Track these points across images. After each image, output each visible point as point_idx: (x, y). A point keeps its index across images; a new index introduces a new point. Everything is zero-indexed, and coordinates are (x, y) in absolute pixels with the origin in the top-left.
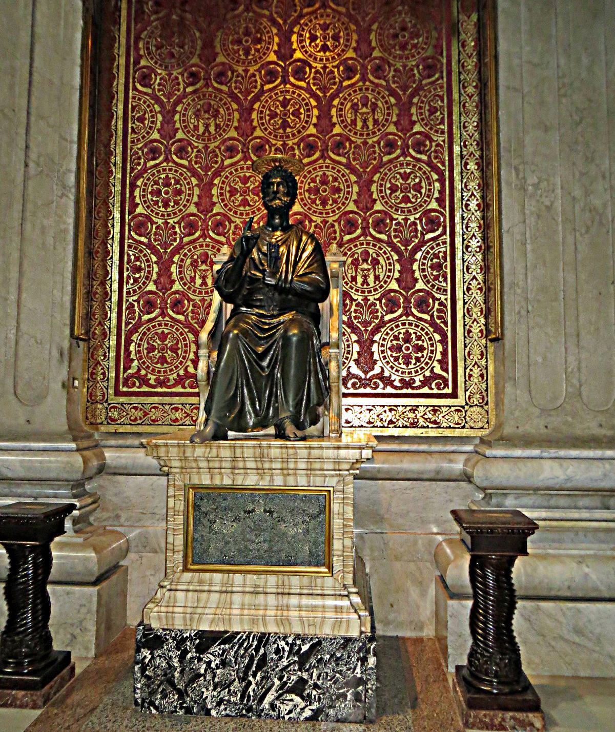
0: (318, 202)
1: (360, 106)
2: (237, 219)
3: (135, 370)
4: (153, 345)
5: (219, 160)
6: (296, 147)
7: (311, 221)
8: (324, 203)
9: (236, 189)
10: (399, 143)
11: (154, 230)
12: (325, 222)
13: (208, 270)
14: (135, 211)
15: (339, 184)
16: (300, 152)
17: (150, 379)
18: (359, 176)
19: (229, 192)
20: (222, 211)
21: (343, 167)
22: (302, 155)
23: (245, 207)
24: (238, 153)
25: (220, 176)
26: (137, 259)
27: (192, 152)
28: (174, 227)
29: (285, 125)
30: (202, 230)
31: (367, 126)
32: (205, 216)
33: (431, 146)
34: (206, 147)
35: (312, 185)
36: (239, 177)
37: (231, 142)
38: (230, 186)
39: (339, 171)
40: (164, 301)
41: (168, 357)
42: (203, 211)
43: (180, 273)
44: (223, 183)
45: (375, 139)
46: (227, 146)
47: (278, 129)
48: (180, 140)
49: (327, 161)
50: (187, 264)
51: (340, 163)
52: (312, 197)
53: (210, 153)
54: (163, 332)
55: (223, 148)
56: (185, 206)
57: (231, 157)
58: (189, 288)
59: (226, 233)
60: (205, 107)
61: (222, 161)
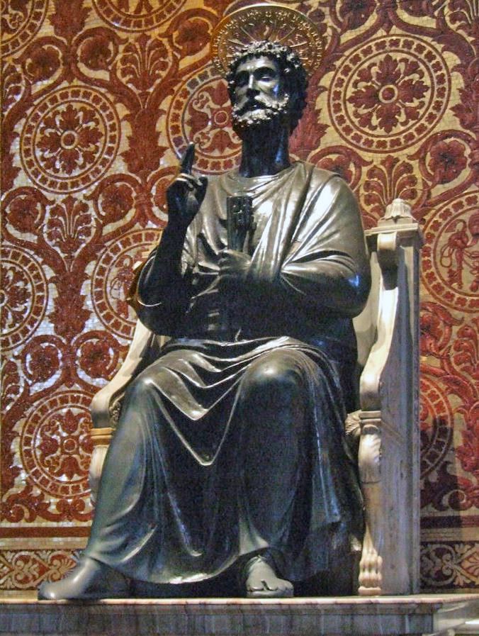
0: (375, 121)
3: (22, 489)
4: (53, 440)
5: (169, 60)
6: (326, 10)
7: (360, 163)
8: (388, 120)
11: (48, 216)
12: (391, 163)
14: (12, 184)
15: (422, 75)
17: (49, 504)
19: (191, 123)
21: (429, 39)
22: (339, 24)
23: (222, 150)
26: (19, 276)
27: (117, 53)
28: (85, 208)
30: (138, 206)
32: (144, 178)
34: (143, 38)
35: (362, 85)
36: (209, 90)
37: (192, 19)
38: (192, 111)
39: (420, 49)
40: (70, 353)
41: (79, 461)
42: (141, 167)
43: (99, 296)
44: (179, 105)
46: (185, 30)
48: (92, 32)
49: (395, 29)
50: (111, 277)
51: (421, 30)
52: (363, 111)
54: (69, 412)
55: (175, 34)
56: (104, 162)
57: (193, 52)
58: (117, 325)
61: (176, 62)
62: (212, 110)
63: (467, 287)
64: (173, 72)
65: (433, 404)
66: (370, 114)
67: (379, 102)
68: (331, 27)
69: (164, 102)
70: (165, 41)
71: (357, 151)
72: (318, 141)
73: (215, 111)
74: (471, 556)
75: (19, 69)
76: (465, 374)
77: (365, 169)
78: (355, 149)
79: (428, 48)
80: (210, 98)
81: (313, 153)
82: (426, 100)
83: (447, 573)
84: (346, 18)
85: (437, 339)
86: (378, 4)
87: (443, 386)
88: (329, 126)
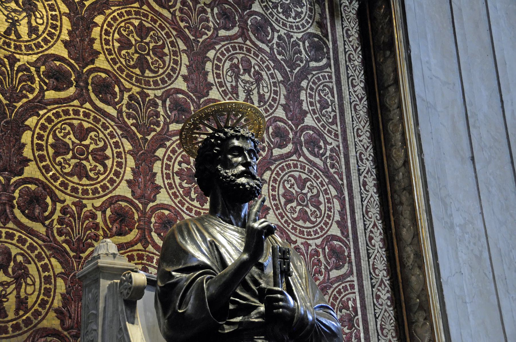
1: (242, 71)
2: (67, 197)
5: (36, 86)
6: (160, 102)
9: (66, 144)
10: (291, 136)
13: (9, 284)
16: (166, 112)
19: (52, 146)
20: (42, 178)
23: (80, 179)
24: (70, 84)
25: (38, 115)
31: (251, 99)
33: (326, 149)
35: (184, 165)
36: (71, 125)
37: (58, 63)
38: (55, 136)
47: (134, 67)
52: (185, 185)
53: (18, 71)
55: (43, 68)
57: (57, 89)
59: (47, 218)
62: (73, 143)
64: (40, 98)
66: (190, 188)
68: (163, 116)
69: (30, 120)
70: (33, 69)
71: (182, 213)
72: (155, 197)
73: (75, 145)
78: (180, 211)
80: (71, 132)
81: (151, 204)
84: (173, 114)
86: (193, 113)
88: (162, 188)
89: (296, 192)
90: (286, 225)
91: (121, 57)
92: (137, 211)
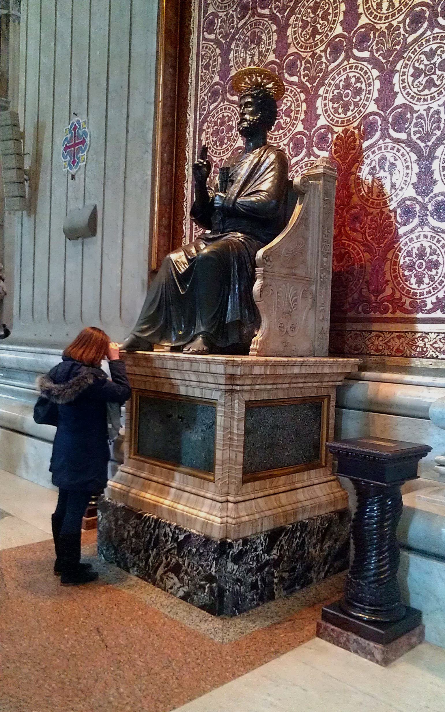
6: (323, 54)
18: (381, 69)
21: (365, 64)
29: (315, 32)
39: (362, 69)
45: (401, 18)
60: (252, 38)
63: (375, 197)
65: (357, 257)
66: (338, 107)
67: (343, 100)
74: (370, 339)
75: (206, 98)
76: (371, 241)
77: (335, 136)
78: (331, 126)
79: (365, 69)
82: (363, 97)
83: (359, 346)
85: (361, 224)
87: (362, 248)
89: (426, 66)
90: (411, 100)
91: (302, 37)
92: (306, 137)
